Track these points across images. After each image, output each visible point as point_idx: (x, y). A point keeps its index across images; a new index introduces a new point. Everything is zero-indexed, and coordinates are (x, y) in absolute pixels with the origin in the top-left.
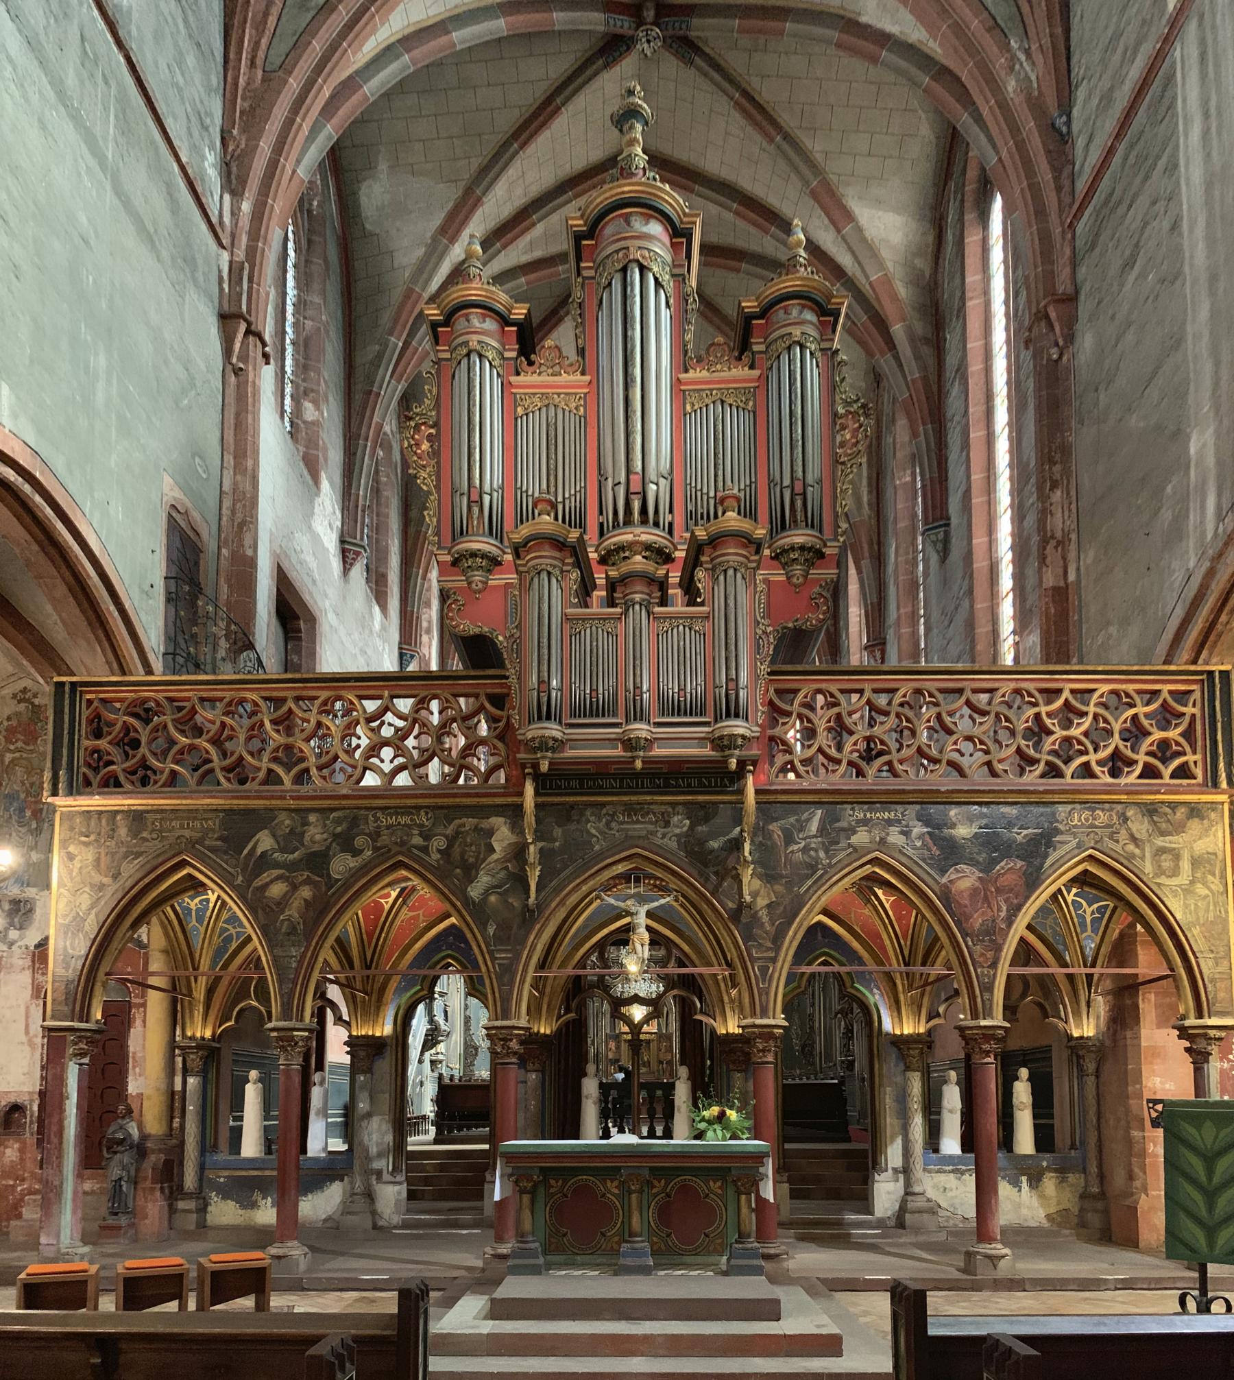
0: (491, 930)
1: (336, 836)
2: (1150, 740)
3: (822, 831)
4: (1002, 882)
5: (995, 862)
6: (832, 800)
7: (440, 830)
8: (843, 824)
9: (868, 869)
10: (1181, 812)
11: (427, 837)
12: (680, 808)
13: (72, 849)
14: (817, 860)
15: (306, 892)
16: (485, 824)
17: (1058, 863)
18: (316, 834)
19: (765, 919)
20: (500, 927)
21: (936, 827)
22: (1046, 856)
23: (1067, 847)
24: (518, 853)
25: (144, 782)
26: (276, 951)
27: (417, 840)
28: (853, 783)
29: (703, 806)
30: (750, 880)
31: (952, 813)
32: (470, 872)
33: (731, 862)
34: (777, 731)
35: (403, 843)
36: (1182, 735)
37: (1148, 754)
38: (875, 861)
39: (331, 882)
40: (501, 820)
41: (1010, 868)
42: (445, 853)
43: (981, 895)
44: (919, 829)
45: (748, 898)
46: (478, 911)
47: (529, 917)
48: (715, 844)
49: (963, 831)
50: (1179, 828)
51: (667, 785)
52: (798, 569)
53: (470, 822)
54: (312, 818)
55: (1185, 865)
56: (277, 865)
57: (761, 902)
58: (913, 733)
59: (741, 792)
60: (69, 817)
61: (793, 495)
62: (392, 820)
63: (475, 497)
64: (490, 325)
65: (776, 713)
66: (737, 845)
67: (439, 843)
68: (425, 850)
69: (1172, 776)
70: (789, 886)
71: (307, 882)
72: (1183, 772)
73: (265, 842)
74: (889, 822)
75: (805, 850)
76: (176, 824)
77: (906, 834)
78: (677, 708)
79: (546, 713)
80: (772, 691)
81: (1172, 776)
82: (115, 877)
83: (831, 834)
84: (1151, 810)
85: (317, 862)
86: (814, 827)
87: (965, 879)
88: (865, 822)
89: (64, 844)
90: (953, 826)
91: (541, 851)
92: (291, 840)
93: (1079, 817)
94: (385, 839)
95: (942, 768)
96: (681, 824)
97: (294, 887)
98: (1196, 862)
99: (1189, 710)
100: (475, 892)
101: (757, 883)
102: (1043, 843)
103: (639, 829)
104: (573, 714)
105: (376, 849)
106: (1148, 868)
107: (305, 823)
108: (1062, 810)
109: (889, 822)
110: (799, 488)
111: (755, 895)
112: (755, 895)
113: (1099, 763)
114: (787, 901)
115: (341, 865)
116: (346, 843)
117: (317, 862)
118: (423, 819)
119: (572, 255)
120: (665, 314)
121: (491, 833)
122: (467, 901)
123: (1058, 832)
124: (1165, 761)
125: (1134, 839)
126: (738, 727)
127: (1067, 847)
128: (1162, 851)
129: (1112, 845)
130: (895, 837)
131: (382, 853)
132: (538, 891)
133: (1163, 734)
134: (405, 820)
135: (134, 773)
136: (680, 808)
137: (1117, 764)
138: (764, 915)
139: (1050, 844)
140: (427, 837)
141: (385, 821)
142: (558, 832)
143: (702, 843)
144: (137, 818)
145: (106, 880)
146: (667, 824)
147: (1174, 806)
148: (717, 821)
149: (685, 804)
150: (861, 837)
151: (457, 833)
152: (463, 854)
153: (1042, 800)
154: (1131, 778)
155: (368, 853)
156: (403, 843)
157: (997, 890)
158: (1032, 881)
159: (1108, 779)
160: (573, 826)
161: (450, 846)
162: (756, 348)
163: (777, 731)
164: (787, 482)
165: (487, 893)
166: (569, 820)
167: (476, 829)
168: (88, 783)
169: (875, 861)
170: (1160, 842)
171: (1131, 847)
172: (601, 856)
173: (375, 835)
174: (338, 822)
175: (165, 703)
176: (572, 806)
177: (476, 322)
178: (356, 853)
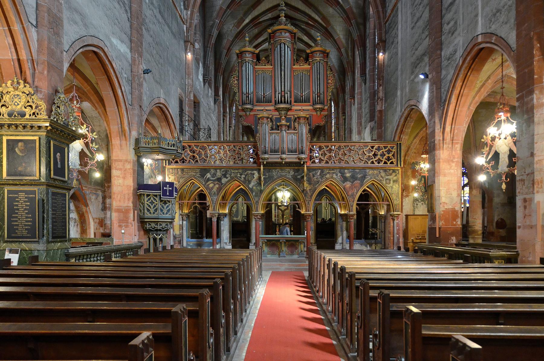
0: (254, 194)
1: (223, 174)
2: (385, 156)
3: (320, 174)
4: (355, 185)
5: (354, 181)
6: (322, 169)
7: (244, 173)
8: (324, 173)
9: (330, 182)
10: (391, 171)
11: (241, 175)
12: (292, 170)
13: (170, 176)
14: (319, 180)
15: (217, 186)
16: (252, 172)
17: (367, 181)
18: (219, 174)
19: (309, 192)
20: (256, 193)
21: (343, 175)
22: (364, 180)
23: (368, 178)
24: (260, 178)
25: (183, 162)
26: (212, 198)
27: (239, 175)
28: (327, 165)
29: (296, 169)
30: (306, 184)
31: (346, 171)
32: (249, 182)
33: (302, 181)
34: (311, 154)
35: (236, 176)
36: (392, 155)
37: (385, 159)
38: (331, 180)
39: (222, 184)
40: (256, 172)
41: (357, 182)
42: (244, 178)
43: (351, 188)
44: (339, 174)
45: (305, 188)
46: (252, 190)
47: (261, 192)
48: (299, 177)
49: (348, 175)
50: (391, 175)
51: (289, 165)
52: (319, 113)
53: (250, 172)
54: (218, 171)
55: (392, 182)
56: (211, 180)
57: (308, 189)
58: (339, 155)
59: (304, 167)
60: (169, 169)
61: (317, 96)
62: (234, 171)
63: (247, 95)
64: (251, 55)
65: (311, 150)
66: (303, 177)
67: (243, 176)
68: (241, 177)
69: (390, 164)
70: (313, 185)
71: (217, 184)
72: (392, 163)
73: (208, 175)
74: (333, 173)
75: (317, 178)
76: (190, 171)
77: (337, 175)
78: (291, 151)
79: (265, 153)
80: (311, 146)
81: (390, 164)
82: (179, 182)
83: (322, 175)
84: (385, 171)
85: (219, 180)
86: (319, 173)
87: (348, 184)
88: (329, 173)
89: (168, 175)
90: (346, 174)
91: (264, 178)
92: (214, 175)
93: (371, 172)
94: (233, 175)
95: (344, 162)
96: (292, 173)
97: (215, 185)
98: (394, 181)
99: (394, 150)
100: (251, 186)
101: (307, 185)
102: (364, 177)
103: (284, 174)
104: (271, 152)
105: (231, 177)
106: (384, 182)
107: (217, 172)
108: (368, 170)
109: (333, 173)
110: (319, 94)
111: (306, 188)
112: (306, 188)
113: (376, 161)
114: (313, 189)
115: (224, 180)
116: (225, 176)
117: (219, 180)
118: (240, 171)
119: (269, 38)
120: (289, 52)
121: (254, 174)
122: (249, 188)
123: (367, 175)
124: (388, 161)
125: (382, 177)
126: (303, 156)
127: (368, 178)
128: (387, 179)
129: (377, 178)
130: (335, 176)
131: (232, 178)
132: (263, 186)
133: (388, 155)
134: (237, 171)
135: (181, 160)
136: (292, 170)
137: (379, 161)
138: (308, 191)
139: (365, 178)
140: (241, 175)
141: (233, 171)
142: (267, 174)
143: (296, 176)
144: (182, 170)
145: (177, 183)
146: (289, 173)
147: (390, 170)
148: (300, 172)
149: (293, 169)
150: (328, 176)
151: (247, 174)
152: (248, 178)
153: (364, 168)
154: (382, 164)
155: (229, 178)
156: (236, 176)
157: (355, 187)
158: (362, 185)
159: (377, 164)
160: (270, 173)
161: (246, 177)
162: (310, 61)
163: (311, 154)
164: (316, 93)
165: (253, 186)
166: (270, 172)
167: (251, 173)
168: (172, 163)
169: (331, 180)
170: (387, 177)
171: (381, 178)
172: (276, 179)
173: (231, 175)
174: (223, 171)
175: (187, 146)
176: (270, 169)
177: (247, 55)
178: (227, 178)
